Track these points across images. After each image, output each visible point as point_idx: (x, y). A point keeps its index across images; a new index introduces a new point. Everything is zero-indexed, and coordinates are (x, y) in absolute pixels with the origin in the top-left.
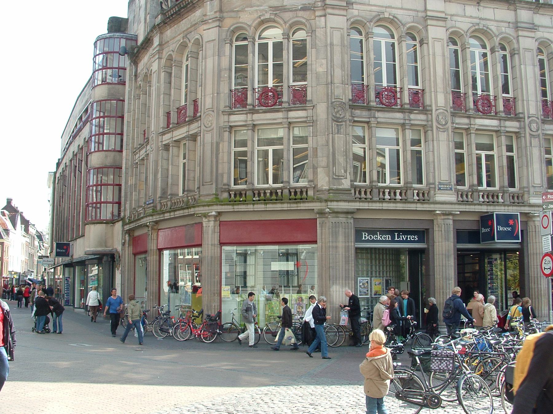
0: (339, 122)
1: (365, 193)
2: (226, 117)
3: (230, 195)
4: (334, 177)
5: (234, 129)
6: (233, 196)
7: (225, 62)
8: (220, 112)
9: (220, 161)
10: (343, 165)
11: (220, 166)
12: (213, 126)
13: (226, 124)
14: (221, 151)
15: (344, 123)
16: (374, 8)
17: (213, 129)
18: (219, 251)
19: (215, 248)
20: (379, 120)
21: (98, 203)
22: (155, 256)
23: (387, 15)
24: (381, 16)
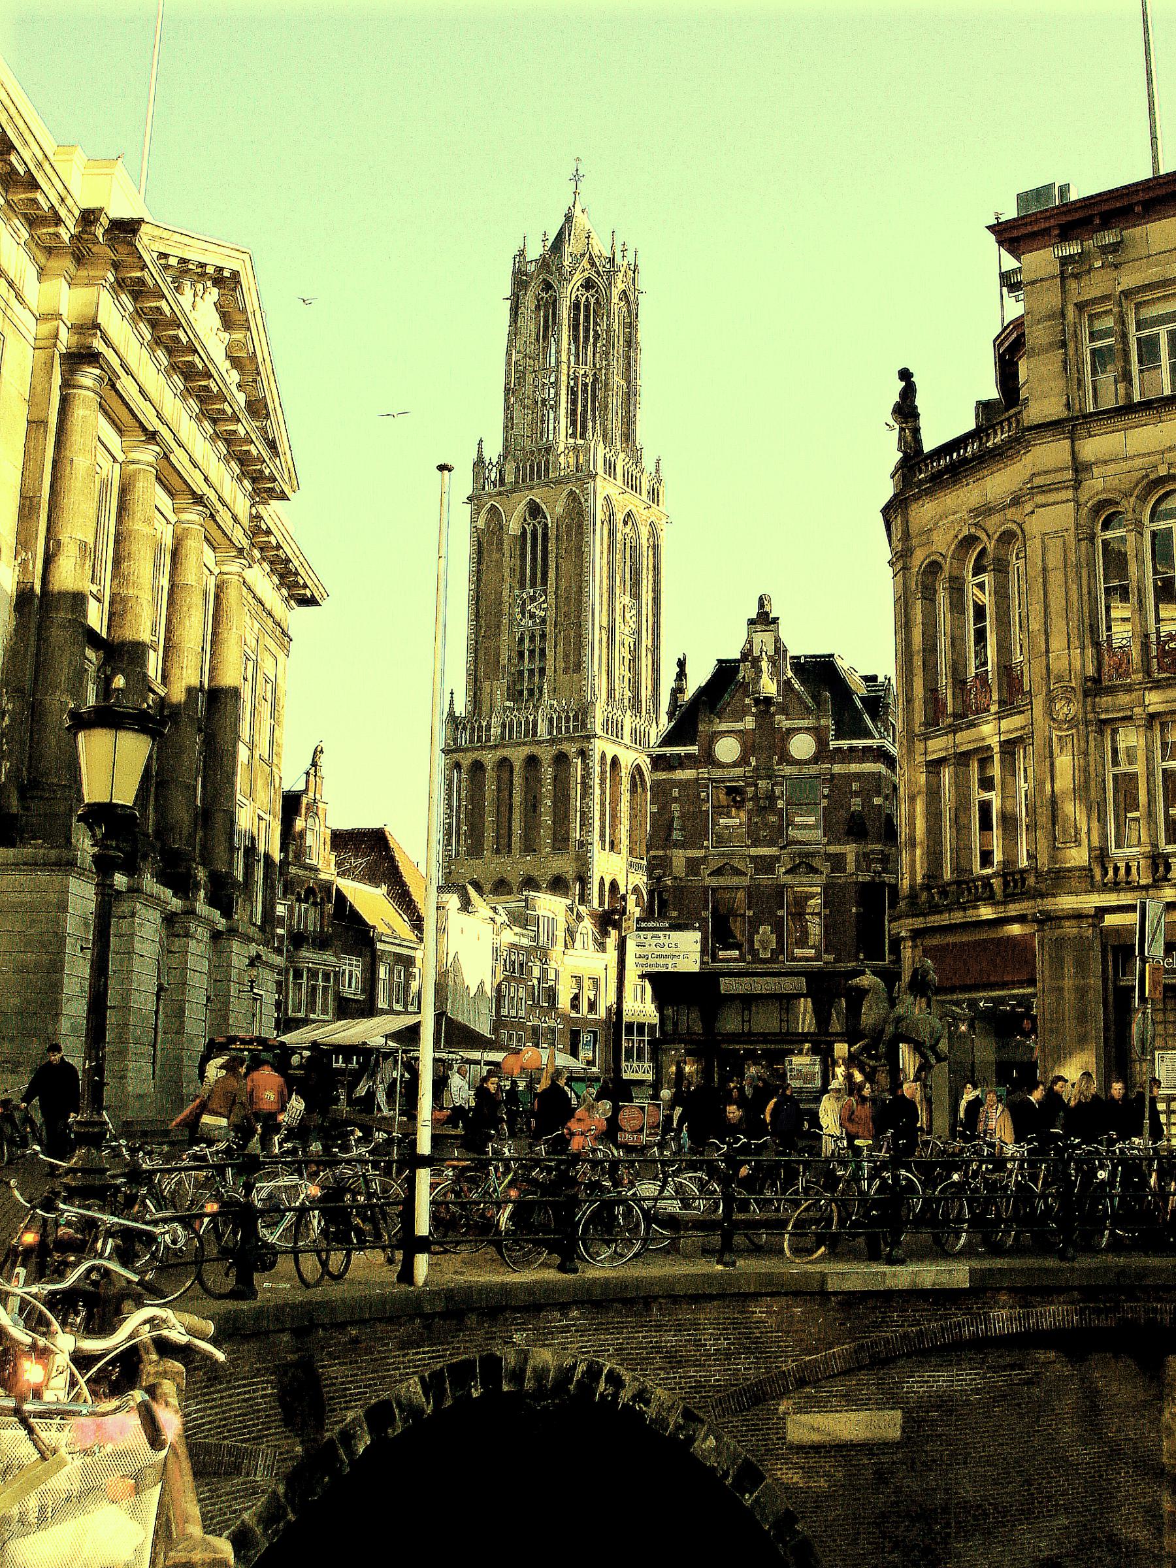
16: (1137, 462)
23: (1162, 471)
24: (1152, 477)
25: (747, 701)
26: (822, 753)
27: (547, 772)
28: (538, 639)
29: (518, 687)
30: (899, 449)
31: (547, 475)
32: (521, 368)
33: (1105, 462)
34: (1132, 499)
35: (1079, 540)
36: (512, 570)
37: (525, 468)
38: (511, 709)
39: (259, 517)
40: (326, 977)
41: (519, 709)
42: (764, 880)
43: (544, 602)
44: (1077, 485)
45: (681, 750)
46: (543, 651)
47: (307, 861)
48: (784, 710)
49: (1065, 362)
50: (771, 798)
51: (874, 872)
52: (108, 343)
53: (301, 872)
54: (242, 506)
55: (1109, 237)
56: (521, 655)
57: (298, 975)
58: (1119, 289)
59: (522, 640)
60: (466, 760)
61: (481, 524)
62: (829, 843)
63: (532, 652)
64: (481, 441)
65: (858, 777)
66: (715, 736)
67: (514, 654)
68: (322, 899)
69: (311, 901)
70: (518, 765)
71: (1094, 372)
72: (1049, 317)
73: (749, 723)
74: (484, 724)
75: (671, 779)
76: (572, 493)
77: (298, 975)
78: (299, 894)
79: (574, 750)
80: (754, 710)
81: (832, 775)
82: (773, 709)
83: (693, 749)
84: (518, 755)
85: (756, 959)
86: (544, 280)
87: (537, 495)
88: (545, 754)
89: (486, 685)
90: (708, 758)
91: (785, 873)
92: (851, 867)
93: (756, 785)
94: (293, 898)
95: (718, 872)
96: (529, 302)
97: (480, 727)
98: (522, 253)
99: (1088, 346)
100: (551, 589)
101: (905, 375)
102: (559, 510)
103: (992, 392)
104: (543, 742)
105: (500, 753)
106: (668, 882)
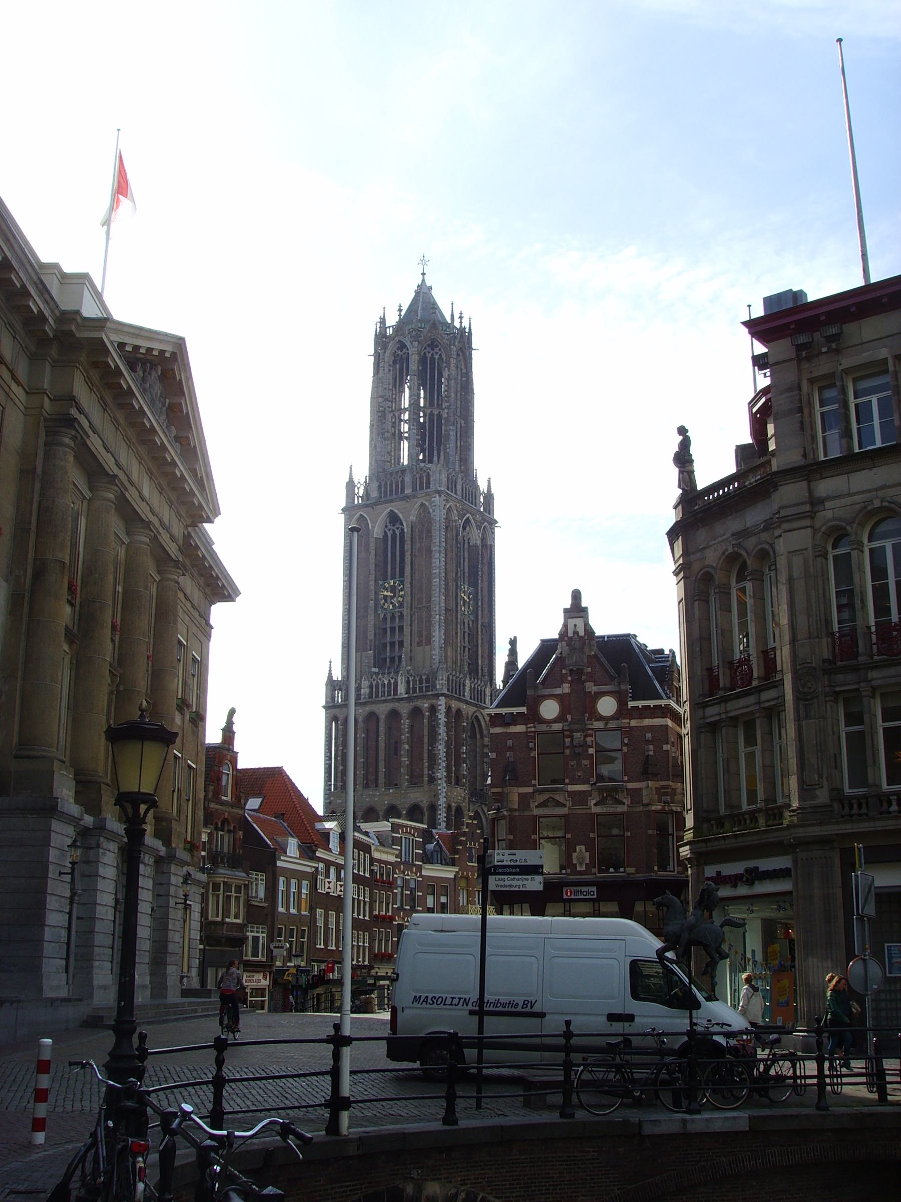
0: (808, 700)
1: (860, 807)
4: (805, 787)
10: (816, 767)
15: (815, 700)
16: (857, 498)
20: (875, 683)
23: (877, 504)
24: (869, 508)
25: (564, 671)
26: (622, 711)
27: (405, 723)
30: (679, 487)
31: (403, 492)
33: (835, 498)
34: (855, 525)
35: (816, 557)
37: (386, 485)
38: (377, 674)
39: (189, 535)
40: (238, 890)
41: (383, 674)
42: (580, 810)
44: (812, 515)
45: (515, 710)
46: (401, 628)
47: (224, 798)
48: (591, 678)
49: (802, 422)
51: (665, 802)
52: (81, 411)
53: (217, 807)
54: (178, 530)
55: (833, 330)
56: (385, 630)
57: (216, 887)
58: (840, 368)
59: (385, 618)
63: (393, 629)
65: (651, 728)
66: (540, 699)
68: (234, 827)
69: (226, 829)
70: (382, 717)
71: (824, 431)
72: (790, 389)
73: (566, 688)
76: (422, 504)
77: (216, 887)
78: (217, 824)
79: (426, 705)
80: (569, 678)
81: (630, 727)
83: (523, 709)
84: (382, 710)
85: (575, 872)
86: (399, 341)
87: (396, 507)
90: (534, 716)
91: (595, 805)
93: (572, 737)
94: (212, 827)
95: (543, 805)
96: (388, 356)
98: (383, 321)
99: (818, 410)
100: (407, 579)
101: (682, 431)
102: (413, 518)
103: (748, 440)
104: (402, 699)
105: (368, 709)
106: (505, 813)
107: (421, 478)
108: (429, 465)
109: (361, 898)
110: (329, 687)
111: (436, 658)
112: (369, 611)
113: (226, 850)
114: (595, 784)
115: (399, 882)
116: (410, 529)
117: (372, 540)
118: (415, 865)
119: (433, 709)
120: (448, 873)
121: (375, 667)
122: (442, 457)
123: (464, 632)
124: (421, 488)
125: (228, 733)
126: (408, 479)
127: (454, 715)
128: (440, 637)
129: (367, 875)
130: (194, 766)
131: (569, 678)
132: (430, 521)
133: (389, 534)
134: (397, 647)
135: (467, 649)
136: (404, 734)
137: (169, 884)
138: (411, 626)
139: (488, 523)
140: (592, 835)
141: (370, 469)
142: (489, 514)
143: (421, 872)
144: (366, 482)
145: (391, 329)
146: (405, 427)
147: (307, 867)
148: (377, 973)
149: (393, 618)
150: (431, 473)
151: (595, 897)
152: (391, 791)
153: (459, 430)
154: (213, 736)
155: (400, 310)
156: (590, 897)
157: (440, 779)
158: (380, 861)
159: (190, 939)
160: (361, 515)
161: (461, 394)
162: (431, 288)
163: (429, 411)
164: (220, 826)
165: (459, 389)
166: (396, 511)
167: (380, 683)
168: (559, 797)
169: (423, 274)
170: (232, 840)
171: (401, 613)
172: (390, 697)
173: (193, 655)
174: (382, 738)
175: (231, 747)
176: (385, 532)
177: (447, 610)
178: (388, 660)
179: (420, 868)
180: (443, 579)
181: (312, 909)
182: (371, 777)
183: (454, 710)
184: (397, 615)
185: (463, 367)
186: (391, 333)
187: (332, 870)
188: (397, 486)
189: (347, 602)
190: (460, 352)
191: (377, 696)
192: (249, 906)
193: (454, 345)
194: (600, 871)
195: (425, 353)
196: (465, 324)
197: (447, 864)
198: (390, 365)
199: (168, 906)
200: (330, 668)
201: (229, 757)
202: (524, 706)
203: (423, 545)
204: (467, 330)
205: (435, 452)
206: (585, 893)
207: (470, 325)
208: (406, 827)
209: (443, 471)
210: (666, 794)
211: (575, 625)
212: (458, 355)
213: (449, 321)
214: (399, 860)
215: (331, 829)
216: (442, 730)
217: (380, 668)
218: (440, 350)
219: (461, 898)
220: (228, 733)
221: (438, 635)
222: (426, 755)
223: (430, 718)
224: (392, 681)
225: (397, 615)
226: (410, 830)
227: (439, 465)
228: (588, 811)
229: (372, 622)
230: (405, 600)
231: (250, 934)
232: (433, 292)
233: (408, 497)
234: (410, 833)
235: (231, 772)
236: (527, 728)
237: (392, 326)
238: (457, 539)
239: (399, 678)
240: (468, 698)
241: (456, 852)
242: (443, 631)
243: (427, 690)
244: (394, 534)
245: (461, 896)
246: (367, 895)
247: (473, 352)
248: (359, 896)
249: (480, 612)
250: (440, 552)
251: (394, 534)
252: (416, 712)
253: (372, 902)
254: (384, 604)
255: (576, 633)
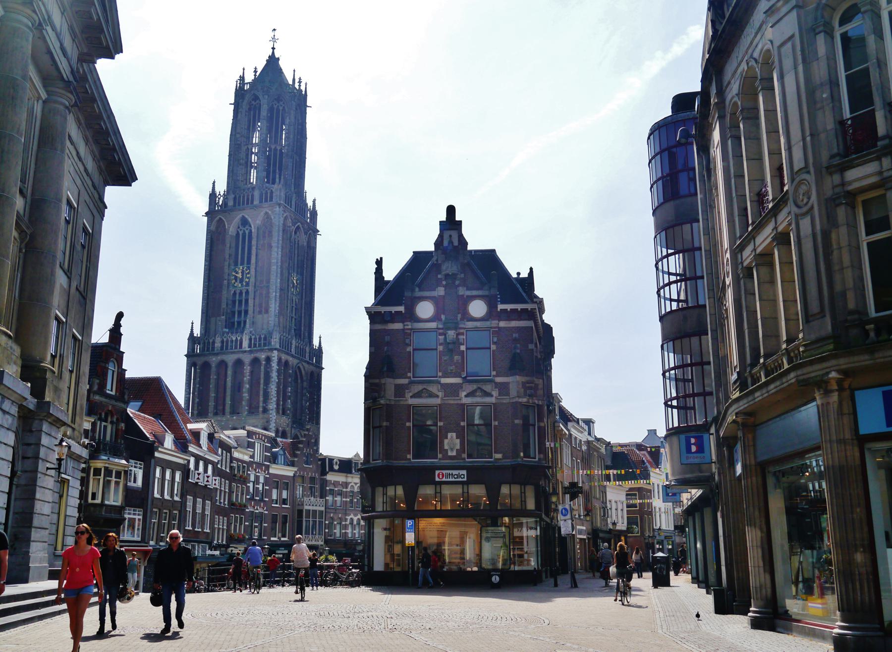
2: (837, 178)
3: (867, 333)
5: (860, 198)
6: (872, 334)
7: (820, 71)
8: (824, 170)
9: (836, 268)
11: (837, 277)
12: (811, 202)
13: (838, 190)
14: (835, 246)
17: (812, 208)
18: (857, 454)
19: (848, 447)
21: (689, 396)
22: (754, 478)
26: (492, 313)
27: (247, 369)
28: (244, 295)
29: (232, 321)
31: (252, 203)
32: (238, 142)
36: (230, 255)
40: (118, 474)
43: (248, 273)
46: (247, 301)
47: (108, 392)
50: (457, 343)
51: (529, 396)
53: (103, 399)
56: (234, 302)
59: (235, 293)
60: (200, 361)
61: (213, 228)
62: (497, 376)
64: (214, 182)
67: (230, 302)
68: (117, 419)
69: (109, 419)
70: (230, 364)
74: (211, 341)
75: (385, 329)
76: (266, 213)
78: (101, 415)
79: (263, 356)
80: (444, 283)
81: (499, 328)
82: (457, 282)
83: (401, 309)
84: (230, 359)
85: (446, 457)
86: (254, 94)
88: (247, 359)
89: (213, 320)
91: (466, 396)
92: (513, 391)
93: (445, 335)
96: (245, 106)
97: (209, 342)
98: (242, 78)
100: (253, 267)
102: (258, 222)
104: (245, 352)
105: (219, 358)
107: (266, 193)
108: (273, 186)
109: (223, 489)
110: (190, 341)
111: (272, 323)
112: (224, 287)
113: (108, 438)
114: (466, 377)
115: (252, 478)
116: (256, 230)
117: (227, 236)
118: (264, 465)
119: (268, 359)
120: (289, 472)
121: (226, 328)
122: (282, 180)
123: (292, 307)
124: (266, 201)
125: (116, 333)
126: (257, 194)
127: (283, 364)
128: (275, 308)
129: (228, 470)
130: (80, 338)
131: (444, 283)
132: (271, 225)
133: (241, 233)
134: (243, 314)
135: (293, 320)
136: (245, 376)
137: (38, 444)
138: (254, 299)
139: (313, 232)
140: (462, 424)
141: (228, 187)
142: (314, 224)
143: (268, 470)
144: (224, 194)
145: (248, 85)
146: (254, 158)
147: (178, 458)
148: (232, 551)
149: (241, 293)
150: (274, 190)
151: (465, 479)
152: (235, 417)
153: (294, 162)
154: (100, 335)
155: (255, 72)
156: (460, 479)
157: (272, 410)
158: (238, 460)
159: (66, 516)
160: (220, 219)
161: (297, 138)
162: (278, 59)
163: (273, 147)
164: (103, 416)
165: (296, 133)
166: (247, 217)
167: (230, 339)
168: (434, 389)
169: (273, 48)
170: (114, 430)
171: (247, 290)
172: (236, 350)
173: (84, 224)
174: (229, 379)
175: (117, 347)
176: (238, 232)
177: (281, 290)
178: (236, 323)
179: (268, 467)
180: (279, 267)
181: (183, 496)
182: (221, 408)
183: (283, 361)
184: (244, 292)
185: (300, 118)
186: (248, 87)
187: (201, 464)
188: (248, 199)
189: (207, 280)
190: (298, 107)
191: (227, 348)
192: (127, 490)
193: (294, 101)
194: (469, 456)
195: (272, 105)
196: (303, 88)
197: (289, 465)
198: (246, 111)
199: (36, 471)
200: (192, 327)
201: (115, 355)
202: (401, 305)
203: (265, 242)
204: (303, 93)
205: (277, 176)
206: (456, 476)
207: (306, 89)
208: (259, 434)
209: (283, 190)
210: (530, 388)
211: (450, 236)
212: (296, 109)
213: (291, 82)
214: (252, 460)
215: (202, 429)
216: (274, 375)
217: (229, 328)
218: (284, 103)
219: (298, 492)
220: (116, 333)
221: (274, 307)
222: (261, 393)
223: (266, 365)
224: (239, 338)
225: (244, 292)
226: (262, 437)
227: (280, 186)
228: (459, 402)
229: (226, 296)
230: (251, 280)
231: (127, 516)
232: (280, 62)
233: (256, 206)
234: (262, 439)
235: (116, 370)
236: (404, 325)
237: (249, 83)
238: (290, 239)
239: (244, 336)
240: (294, 353)
241: (295, 456)
242: (278, 304)
243: (265, 345)
244: (244, 234)
245: (298, 490)
246: (227, 487)
247: (308, 108)
248: (221, 487)
249: (304, 293)
250: (278, 248)
251: (244, 234)
252: (255, 362)
253: (231, 492)
254: (235, 283)
255: (451, 242)
